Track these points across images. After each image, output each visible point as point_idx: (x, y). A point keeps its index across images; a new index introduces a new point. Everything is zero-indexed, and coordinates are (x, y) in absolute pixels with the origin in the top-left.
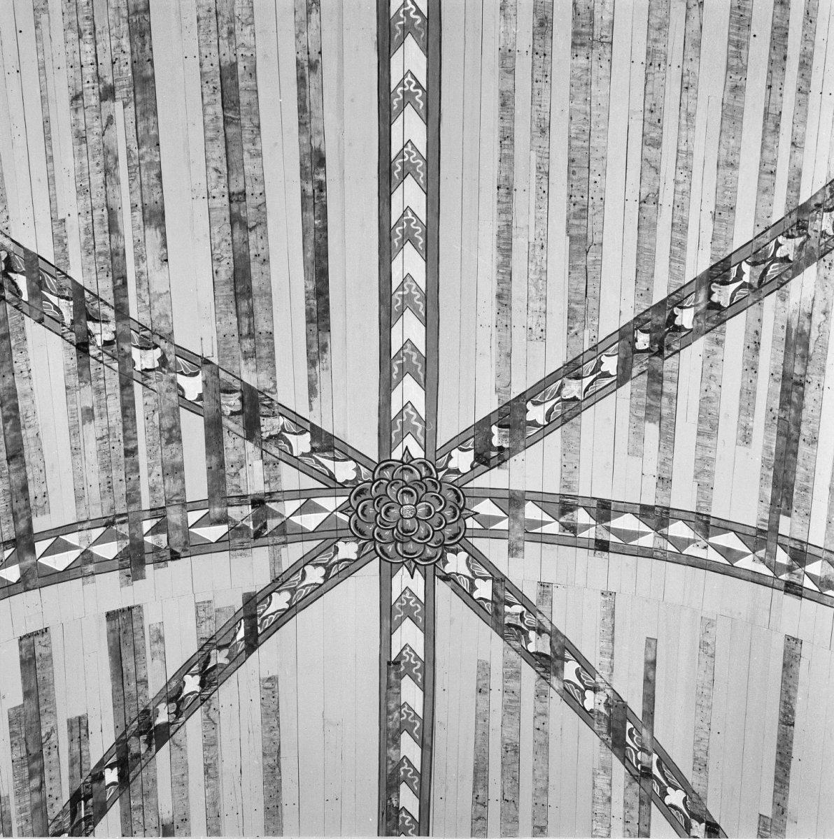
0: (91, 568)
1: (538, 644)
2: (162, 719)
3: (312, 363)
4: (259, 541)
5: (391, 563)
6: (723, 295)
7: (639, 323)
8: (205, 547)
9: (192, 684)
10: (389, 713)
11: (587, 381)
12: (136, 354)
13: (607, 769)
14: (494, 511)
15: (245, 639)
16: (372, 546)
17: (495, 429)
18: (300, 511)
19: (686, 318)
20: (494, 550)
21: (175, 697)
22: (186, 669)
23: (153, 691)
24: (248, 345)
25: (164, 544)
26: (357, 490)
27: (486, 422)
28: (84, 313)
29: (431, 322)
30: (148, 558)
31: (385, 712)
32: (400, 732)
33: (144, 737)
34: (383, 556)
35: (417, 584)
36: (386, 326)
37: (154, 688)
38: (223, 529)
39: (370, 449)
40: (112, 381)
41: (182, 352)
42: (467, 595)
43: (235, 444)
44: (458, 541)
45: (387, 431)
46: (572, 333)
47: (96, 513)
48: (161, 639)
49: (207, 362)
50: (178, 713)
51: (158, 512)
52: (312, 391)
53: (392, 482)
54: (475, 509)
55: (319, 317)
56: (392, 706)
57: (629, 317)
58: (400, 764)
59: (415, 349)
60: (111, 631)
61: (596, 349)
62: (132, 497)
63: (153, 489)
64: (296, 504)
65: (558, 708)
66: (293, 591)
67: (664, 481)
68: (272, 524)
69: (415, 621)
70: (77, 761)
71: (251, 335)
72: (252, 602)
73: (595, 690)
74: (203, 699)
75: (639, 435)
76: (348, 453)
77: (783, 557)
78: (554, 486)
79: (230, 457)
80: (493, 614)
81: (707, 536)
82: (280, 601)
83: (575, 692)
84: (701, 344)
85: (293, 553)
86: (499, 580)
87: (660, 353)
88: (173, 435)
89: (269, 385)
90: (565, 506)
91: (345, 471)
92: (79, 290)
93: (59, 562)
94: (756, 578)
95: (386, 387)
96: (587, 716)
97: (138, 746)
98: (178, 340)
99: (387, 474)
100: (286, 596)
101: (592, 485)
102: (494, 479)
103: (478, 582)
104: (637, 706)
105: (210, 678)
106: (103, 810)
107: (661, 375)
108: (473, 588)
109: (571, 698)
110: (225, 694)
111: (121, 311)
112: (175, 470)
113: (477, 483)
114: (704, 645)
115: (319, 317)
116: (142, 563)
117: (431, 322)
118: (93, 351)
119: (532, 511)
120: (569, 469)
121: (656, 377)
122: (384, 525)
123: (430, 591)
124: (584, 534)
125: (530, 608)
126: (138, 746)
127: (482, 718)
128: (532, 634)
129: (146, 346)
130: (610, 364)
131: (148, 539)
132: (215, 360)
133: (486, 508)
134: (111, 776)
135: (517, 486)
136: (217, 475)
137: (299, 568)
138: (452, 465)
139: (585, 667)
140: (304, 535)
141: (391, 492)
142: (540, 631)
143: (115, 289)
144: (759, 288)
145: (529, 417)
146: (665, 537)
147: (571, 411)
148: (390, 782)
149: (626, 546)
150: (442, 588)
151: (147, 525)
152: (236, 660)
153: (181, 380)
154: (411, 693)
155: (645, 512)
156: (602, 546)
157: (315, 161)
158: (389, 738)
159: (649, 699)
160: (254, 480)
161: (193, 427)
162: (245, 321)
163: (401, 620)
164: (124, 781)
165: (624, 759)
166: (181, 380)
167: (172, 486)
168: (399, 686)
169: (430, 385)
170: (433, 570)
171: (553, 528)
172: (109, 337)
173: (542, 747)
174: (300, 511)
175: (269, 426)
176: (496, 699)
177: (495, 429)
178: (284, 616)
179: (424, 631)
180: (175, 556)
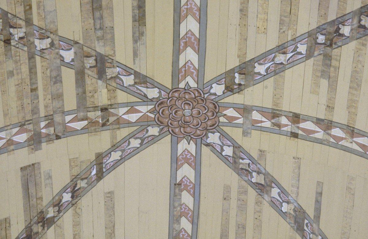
0: (12, 147)
2: (51, 214)
3: (135, 41)
4: (105, 128)
5: (178, 137)
7: (320, 30)
8: (75, 132)
9: (67, 197)
10: (174, 207)
11: (289, 55)
12: (37, 42)
14: (236, 114)
15: (96, 174)
17: (237, 75)
18: (127, 113)
19: (346, 30)
20: (236, 134)
21: (58, 205)
22: (64, 190)
23: (45, 202)
24: (99, 33)
25: (52, 132)
26: (159, 102)
27: (232, 71)
29: (202, 21)
30: (43, 140)
31: (172, 207)
32: (181, 216)
33: (41, 224)
34: (173, 133)
35: (192, 147)
36: (177, 22)
37: (47, 199)
38: (85, 123)
39: (168, 83)
40: (24, 57)
41: (62, 39)
42: (219, 154)
43: (91, 81)
44: (215, 127)
46: (281, 32)
47: (15, 120)
48: (50, 177)
49: (76, 43)
50: (59, 211)
51: (50, 118)
52: (135, 54)
53: (179, 98)
54: (225, 112)
56: (176, 204)
57: (314, 26)
58: (181, 231)
59: (193, 34)
60: (23, 176)
62: (35, 111)
63: (46, 107)
64: (126, 109)
65: (268, 211)
66: (123, 151)
67: (330, 108)
68: (112, 119)
69: (190, 165)
71: (101, 28)
72: (100, 158)
73: (288, 203)
74: (73, 204)
75: (317, 85)
76: (154, 85)
78: (268, 104)
79: (89, 88)
81: (353, 137)
82: (116, 156)
83: (277, 203)
84: (353, 44)
85: (124, 133)
86: (237, 147)
87: (331, 45)
88: (57, 80)
89: (111, 53)
90: (274, 114)
91: (153, 93)
95: (177, 53)
96: (284, 215)
98: (60, 33)
99: (176, 95)
100: (119, 153)
102: (236, 99)
103: (225, 148)
104: (311, 212)
105: (75, 193)
107: (331, 57)
108: (222, 150)
109: (274, 204)
110: (84, 201)
111: (29, 22)
112: (59, 97)
113: (227, 100)
114: (349, 189)
116: (40, 142)
117: (202, 21)
118: (13, 43)
119: (256, 116)
120: (277, 96)
121: (327, 57)
122: (174, 119)
124: (285, 129)
127: (225, 212)
128: (254, 174)
129: (42, 38)
130: (302, 48)
131: (44, 131)
132: (81, 42)
133: (230, 112)
135: (248, 103)
136: (82, 97)
137: (127, 140)
138: (212, 91)
139: (283, 191)
140: (129, 124)
141: (178, 103)
142: (259, 173)
143: (25, 11)
145: (256, 70)
146: (329, 134)
147: (279, 69)
150: (205, 149)
151: (43, 124)
152: (91, 185)
153: (62, 53)
154: (187, 199)
155: (318, 122)
156: (295, 135)
158: (174, 219)
159: (318, 210)
160: (103, 98)
162: (98, 22)
163: (182, 164)
166: (62, 53)
167: (57, 104)
168: (181, 195)
169: (201, 51)
171: (267, 124)
172: (22, 35)
173: (258, 227)
174: (127, 113)
175: (110, 72)
176: (234, 203)
177: (237, 75)
178: (117, 164)
179: (195, 169)
180: (58, 137)
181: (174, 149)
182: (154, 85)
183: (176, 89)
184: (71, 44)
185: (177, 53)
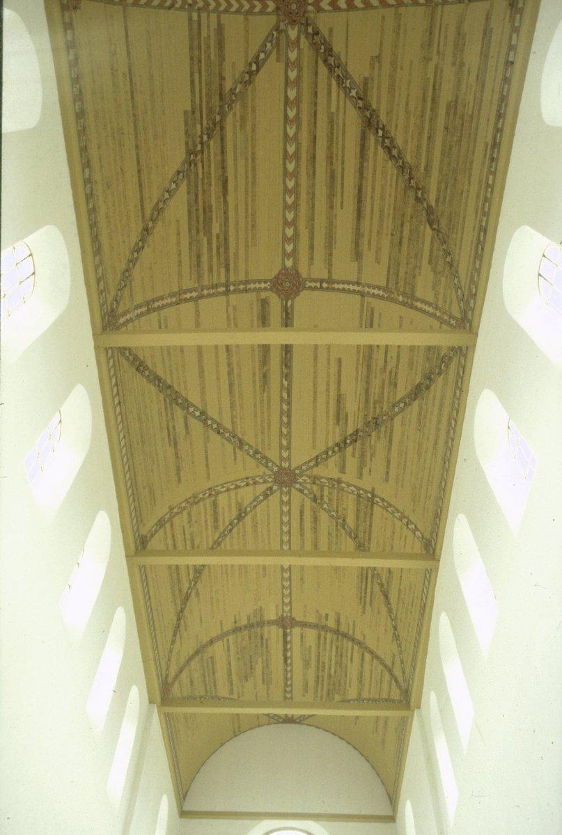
1: (259, 456)
6: (230, 527)
9: (330, 453)
13: (242, 435)
16: (293, 472)
19: (236, 521)
20: (268, 472)
27: (271, 494)
28: (343, 526)
35: (283, 465)
37: (337, 455)
43: (318, 495)
44: (275, 474)
45: (289, 493)
52: (303, 500)
55: (302, 513)
61: (251, 511)
65: (253, 444)
68: (312, 479)
70: (354, 449)
72: (317, 464)
76: (297, 489)
77: (213, 493)
80: (268, 460)
82: (311, 464)
85: (308, 473)
86: (267, 467)
90: (255, 483)
91: (297, 486)
92: (344, 529)
93: (353, 488)
94: (217, 486)
95: (290, 500)
96: (247, 444)
97: (342, 445)
101: (250, 488)
102: (269, 485)
106: (351, 435)
109: (251, 447)
110: (324, 448)
111: (337, 523)
112: (330, 493)
115: (302, 513)
123: (281, 465)
125: (261, 463)
126: (342, 445)
130: (248, 509)
133: (270, 480)
134: (348, 441)
136: (322, 490)
137: (307, 470)
140: (306, 476)
142: (258, 459)
144: (224, 531)
148: (289, 423)
149: (242, 480)
150: (278, 463)
155: (239, 487)
156: (247, 478)
157: (302, 535)
158: (289, 433)
160: (315, 488)
161: (326, 499)
164: (346, 439)
165: (239, 438)
170: (280, 468)
171: (257, 479)
175: (312, 496)
178: (310, 461)
181: (290, 464)
182: (297, 489)
183: (290, 487)
184: (324, 509)
185: (290, 500)
